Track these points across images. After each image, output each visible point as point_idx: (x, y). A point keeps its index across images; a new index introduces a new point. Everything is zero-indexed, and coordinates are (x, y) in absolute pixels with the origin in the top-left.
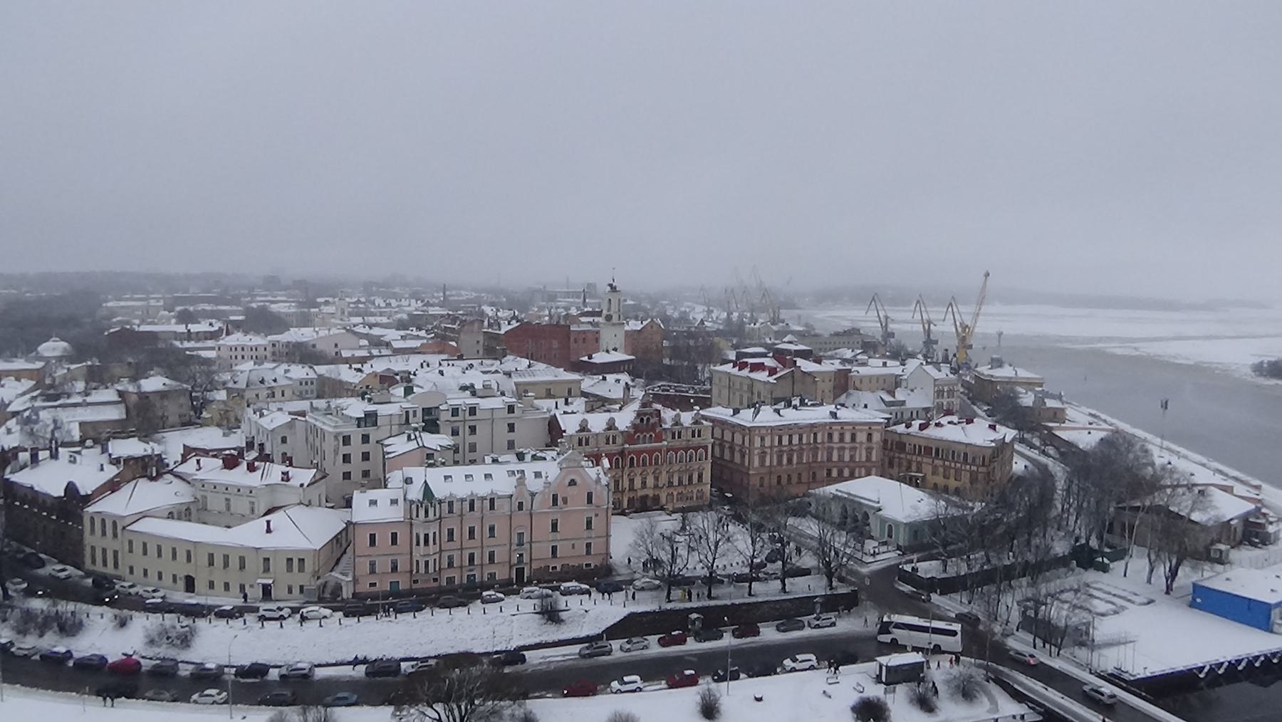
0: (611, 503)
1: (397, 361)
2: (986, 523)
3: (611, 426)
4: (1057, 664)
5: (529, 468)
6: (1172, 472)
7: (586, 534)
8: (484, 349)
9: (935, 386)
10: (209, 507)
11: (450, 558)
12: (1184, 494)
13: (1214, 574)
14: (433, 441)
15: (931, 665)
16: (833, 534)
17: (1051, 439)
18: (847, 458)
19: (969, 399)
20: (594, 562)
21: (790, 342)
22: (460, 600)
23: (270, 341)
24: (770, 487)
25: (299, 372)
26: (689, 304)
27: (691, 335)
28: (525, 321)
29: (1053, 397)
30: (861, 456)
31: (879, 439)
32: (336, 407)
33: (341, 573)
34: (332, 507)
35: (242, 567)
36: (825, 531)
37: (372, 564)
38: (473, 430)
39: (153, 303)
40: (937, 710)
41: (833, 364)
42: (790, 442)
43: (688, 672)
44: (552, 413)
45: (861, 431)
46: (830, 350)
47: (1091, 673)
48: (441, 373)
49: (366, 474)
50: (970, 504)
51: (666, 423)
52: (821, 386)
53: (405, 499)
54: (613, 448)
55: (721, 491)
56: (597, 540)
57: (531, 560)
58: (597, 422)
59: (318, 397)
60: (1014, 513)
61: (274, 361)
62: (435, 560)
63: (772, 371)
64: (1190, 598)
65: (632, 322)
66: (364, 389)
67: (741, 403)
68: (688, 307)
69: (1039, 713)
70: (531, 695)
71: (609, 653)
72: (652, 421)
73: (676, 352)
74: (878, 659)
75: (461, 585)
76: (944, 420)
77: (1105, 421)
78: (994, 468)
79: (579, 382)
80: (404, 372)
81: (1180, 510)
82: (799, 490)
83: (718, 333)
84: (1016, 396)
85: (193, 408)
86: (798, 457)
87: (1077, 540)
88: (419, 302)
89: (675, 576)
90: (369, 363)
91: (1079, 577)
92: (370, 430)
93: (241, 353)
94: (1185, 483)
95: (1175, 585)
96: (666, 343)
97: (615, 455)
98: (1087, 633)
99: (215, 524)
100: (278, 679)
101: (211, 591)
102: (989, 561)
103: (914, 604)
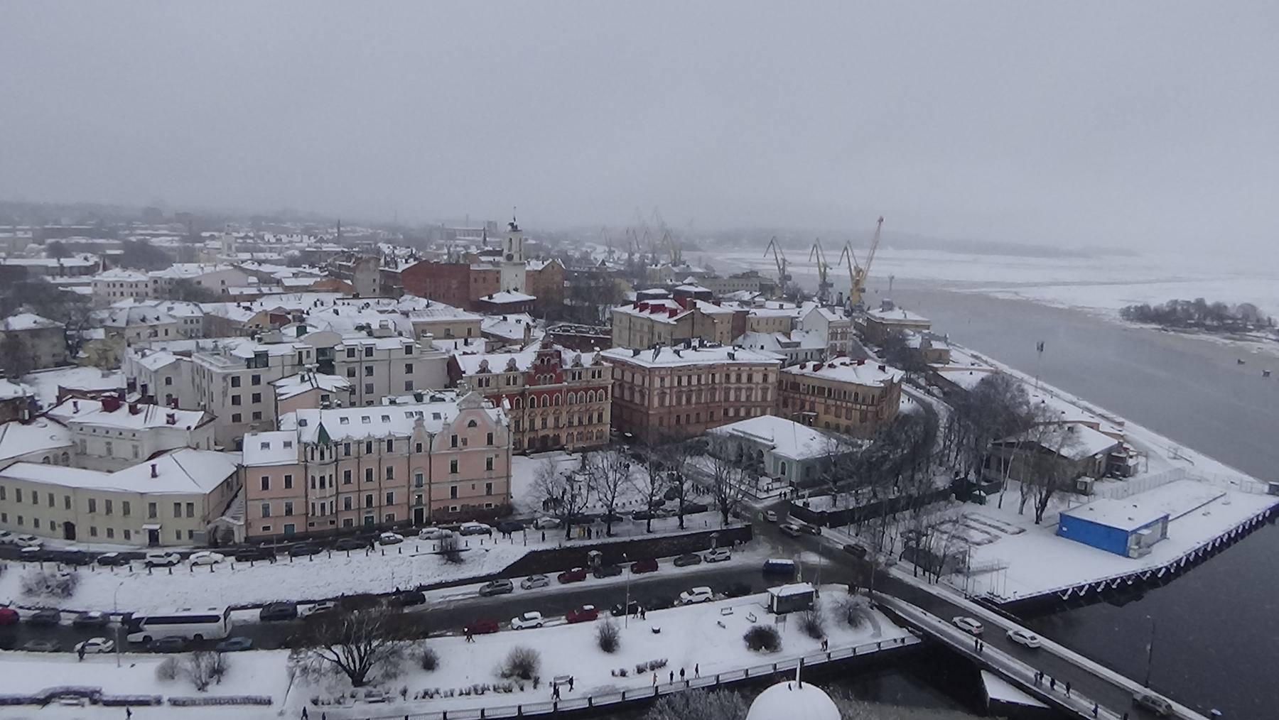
0: (511, 443)
1: (288, 299)
2: (874, 459)
3: (512, 367)
4: (935, 590)
5: (428, 409)
6: (1044, 410)
7: (486, 475)
9: (829, 328)
10: (88, 451)
12: (1054, 431)
13: (1077, 505)
15: (820, 594)
16: (728, 472)
17: (936, 379)
18: (743, 398)
20: (495, 502)
21: (690, 284)
22: (358, 542)
23: (151, 278)
25: (183, 310)
27: (592, 276)
28: (424, 259)
29: (938, 339)
30: (757, 395)
32: (224, 347)
33: (232, 517)
34: (222, 451)
35: (126, 511)
36: (722, 469)
37: (266, 508)
38: (370, 371)
39: (20, 234)
42: (689, 382)
43: (587, 607)
44: (451, 354)
45: (757, 372)
46: (729, 292)
47: (966, 598)
48: (336, 312)
49: (257, 416)
50: (860, 442)
51: (566, 364)
52: (720, 327)
53: (299, 442)
54: (512, 388)
55: (620, 429)
56: (497, 481)
57: (430, 500)
58: (498, 363)
59: (205, 336)
60: (899, 450)
61: (156, 298)
62: (331, 502)
63: (673, 313)
65: (533, 262)
66: (254, 328)
68: (590, 247)
69: (918, 636)
70: (431, 634)
71: (510, 590)
72: (553, 362)
73: (576, 293)
75: (359, 527)
76: (837, 362)
77: (986, 362)
79: (479, 322)
80: (297, 310)
81: (1050, 446)
82: (698, 429)
83: (620, 274)
84: (904, 339)
85: (68, 347)
87: (957, 474)
88: (312, 238)
89: (574, 515)
90: (259, 301)
92: (260, 371)
93: (120, 289)
94: (1056, 420)
96: (567, 284)
98: (964, 562)
99: (96, 469)
101: (93, 538)
102: (875, 495)
103: (806, 540)
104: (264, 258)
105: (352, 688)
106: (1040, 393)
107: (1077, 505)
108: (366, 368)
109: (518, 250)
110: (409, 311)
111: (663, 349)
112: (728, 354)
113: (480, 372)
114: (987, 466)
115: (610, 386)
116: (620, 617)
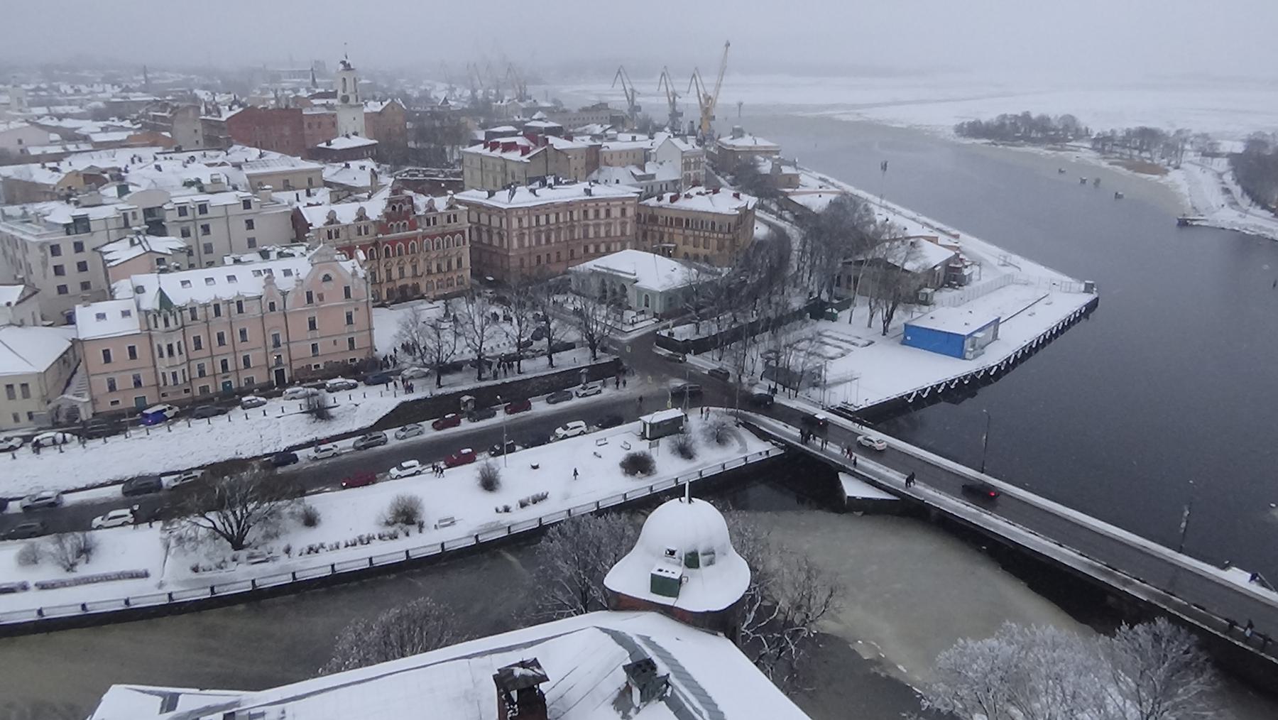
0: (370, 295)
1: (101, 157)
3: (361, 216)
5: (277, 266)
6: (891, 227)
7: (347, 329)
8: (204, 139)
11: (201, 367)
13: (920, 315)
14: (161, 244)
15: (689, 418)
16: (594, 308)
17: (786, 204)
18: (603, 234)
19: (713, 169)
20: (359, 356)
24: (531, 268)
26: (428, 81)
28: (249, 105)
29: (789, 164)
31: (632, 213)
32: (36, 214)
33: (74, 395)
38: (206, 229)
40: (695, 456)
41: (583, 140)
43: (464, 451)
44: (295, 206)
45: (615, 206)
46: (580, 126)
48: (158, 168)
49: (85, 286)
50: (719, 270)
51: (419, 210)
52: (573, 163)
53: (139, 310)
54: (367, 239)
56: (360, 334)
57: (290, 360)
58: (346, 213)
60: (757, 275)
62: (183, 370)
63: (525, 151)
64: (902, 336)
65: (371, 103)
67: (495, 185)
68: (429, 85)
70: (308, 492)
71: (385, 442)
72: (405, 208)
74: (641, 418)
75: (217, 394)
76: (693, 191)
79: (320, 171)
82: (560, 268)
83: (463, 112)
84: (755, 165)
86: (556, 237)
87: (811, 294)
88: (116, 87)
90: (67, 161)
91: (813, 327)
95: (890, 326)
96: (409, 125)
97: (369, 246)
98: (820, 376)
100: (20, 511)
102: (735, 320)
103: (673, 366)
104: (63, 112)
105: (234, 552)
106: (883, 211)
107: (920, 315)
108: (202, 226)
109: (353, 90)
110: (242, 163)
111: (518, 188)
112: (585, 190)
113: (328, 223)
114: (838, 285)
116: (498, 457)
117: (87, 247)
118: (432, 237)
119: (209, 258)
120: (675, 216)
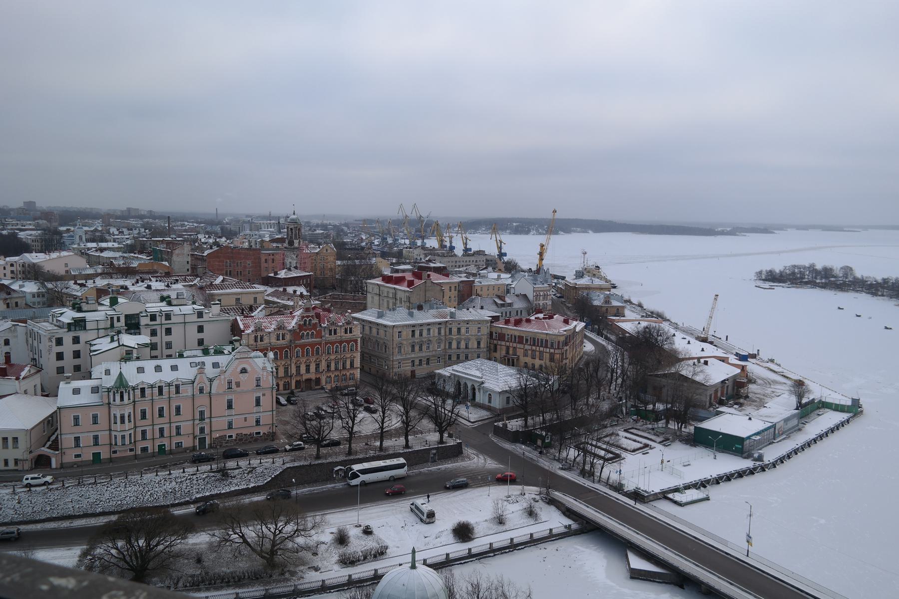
37: (77, 439)
38: (168, 331)
52: (447, 294)
57: (211, 431)
62: (130, 434)
72: (313, 322)
78: (566, 350)
97: (284, 348)
115: (359, 339)
117: (82, 340)
118: (333, 343)
119: (169, 352)
120: (518, 335)
